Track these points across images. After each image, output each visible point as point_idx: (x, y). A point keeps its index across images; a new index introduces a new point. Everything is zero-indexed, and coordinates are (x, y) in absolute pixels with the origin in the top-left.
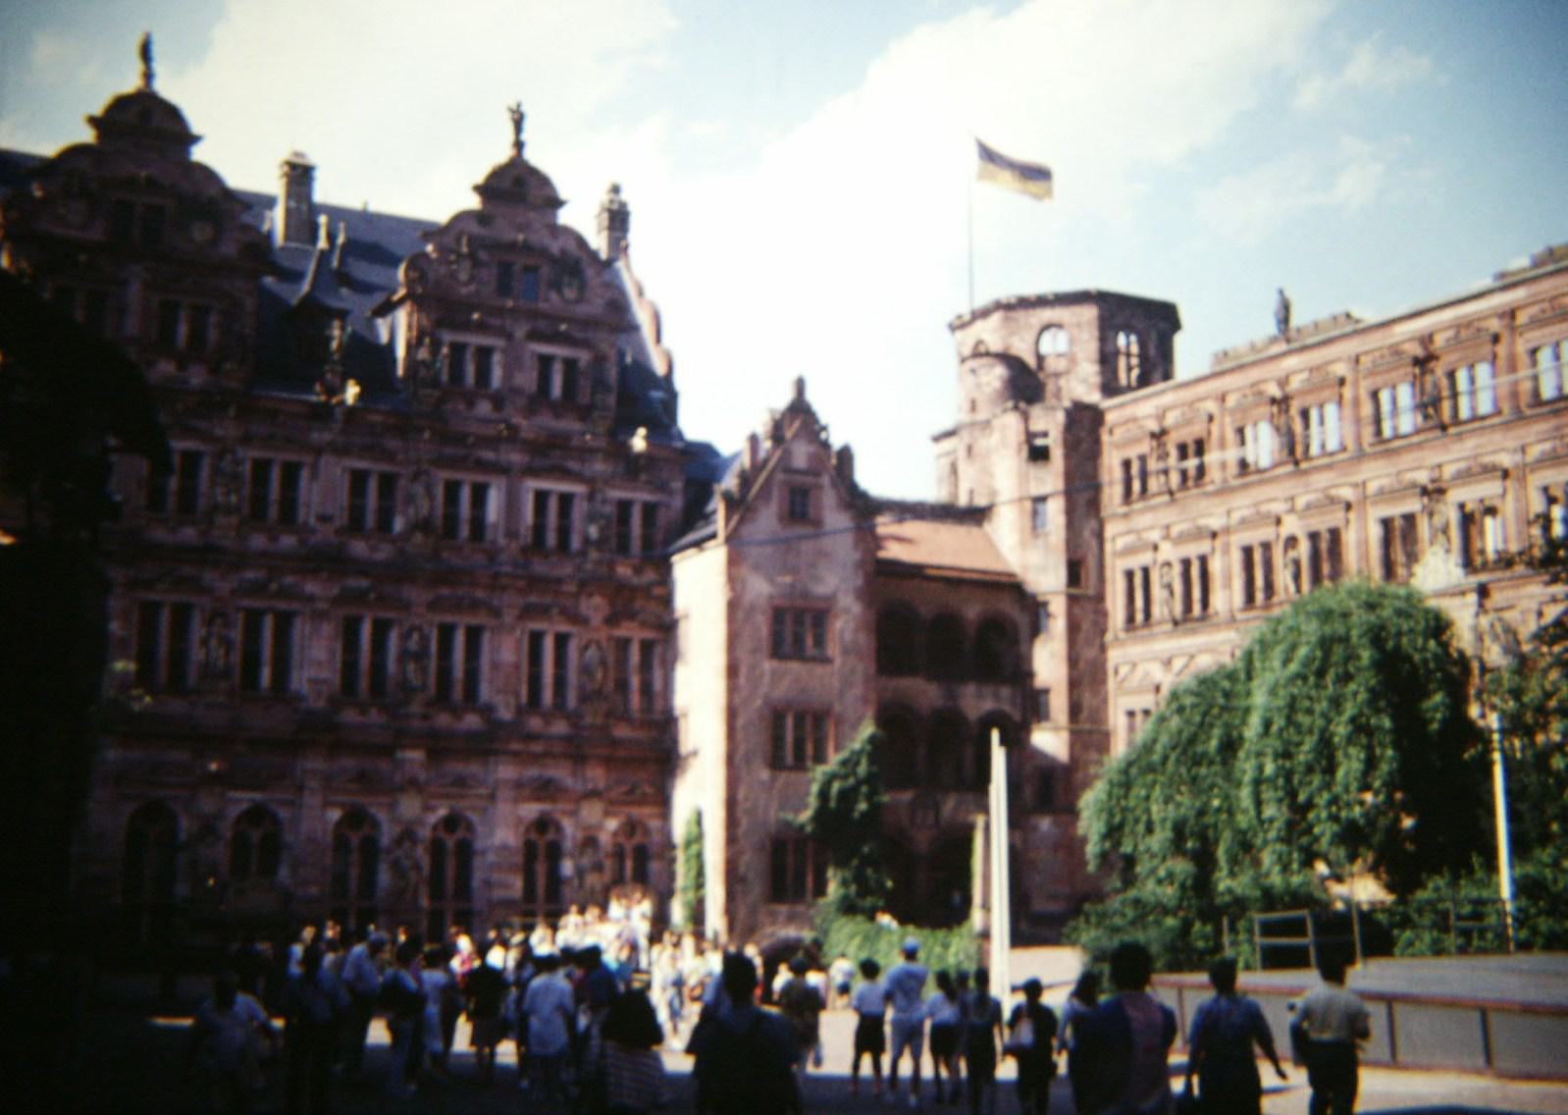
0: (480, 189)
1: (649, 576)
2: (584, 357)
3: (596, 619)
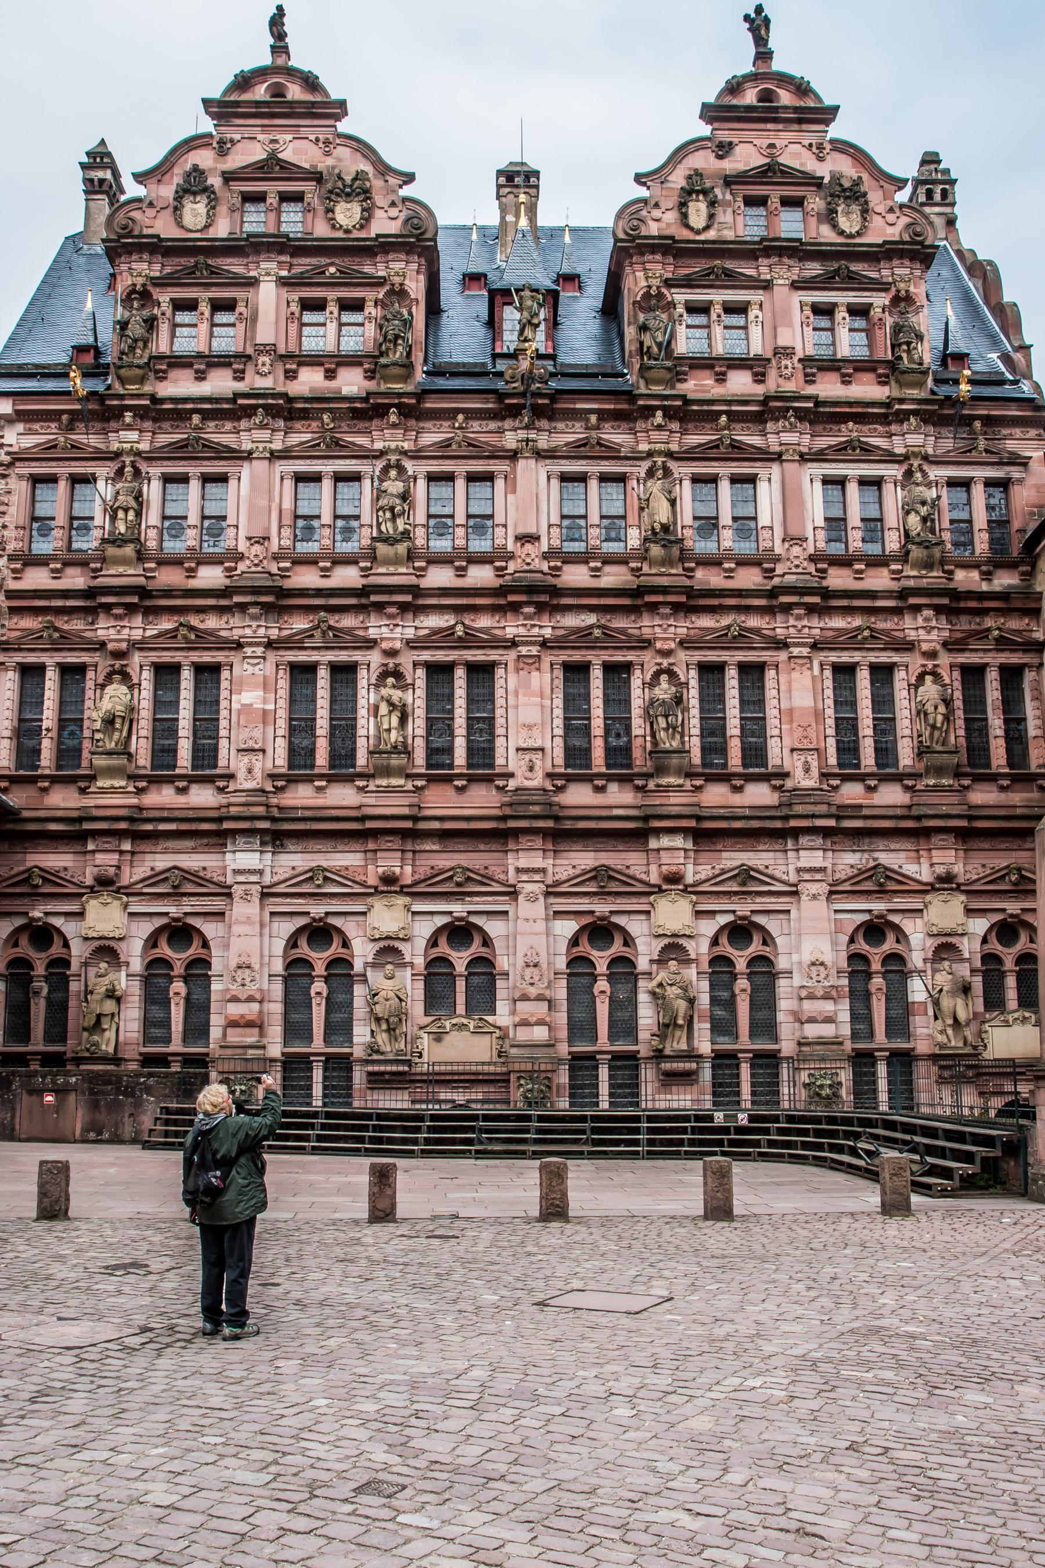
0: (711, 113)
1: (1005, 580)
2: (879, 300)
3: (930, 640)
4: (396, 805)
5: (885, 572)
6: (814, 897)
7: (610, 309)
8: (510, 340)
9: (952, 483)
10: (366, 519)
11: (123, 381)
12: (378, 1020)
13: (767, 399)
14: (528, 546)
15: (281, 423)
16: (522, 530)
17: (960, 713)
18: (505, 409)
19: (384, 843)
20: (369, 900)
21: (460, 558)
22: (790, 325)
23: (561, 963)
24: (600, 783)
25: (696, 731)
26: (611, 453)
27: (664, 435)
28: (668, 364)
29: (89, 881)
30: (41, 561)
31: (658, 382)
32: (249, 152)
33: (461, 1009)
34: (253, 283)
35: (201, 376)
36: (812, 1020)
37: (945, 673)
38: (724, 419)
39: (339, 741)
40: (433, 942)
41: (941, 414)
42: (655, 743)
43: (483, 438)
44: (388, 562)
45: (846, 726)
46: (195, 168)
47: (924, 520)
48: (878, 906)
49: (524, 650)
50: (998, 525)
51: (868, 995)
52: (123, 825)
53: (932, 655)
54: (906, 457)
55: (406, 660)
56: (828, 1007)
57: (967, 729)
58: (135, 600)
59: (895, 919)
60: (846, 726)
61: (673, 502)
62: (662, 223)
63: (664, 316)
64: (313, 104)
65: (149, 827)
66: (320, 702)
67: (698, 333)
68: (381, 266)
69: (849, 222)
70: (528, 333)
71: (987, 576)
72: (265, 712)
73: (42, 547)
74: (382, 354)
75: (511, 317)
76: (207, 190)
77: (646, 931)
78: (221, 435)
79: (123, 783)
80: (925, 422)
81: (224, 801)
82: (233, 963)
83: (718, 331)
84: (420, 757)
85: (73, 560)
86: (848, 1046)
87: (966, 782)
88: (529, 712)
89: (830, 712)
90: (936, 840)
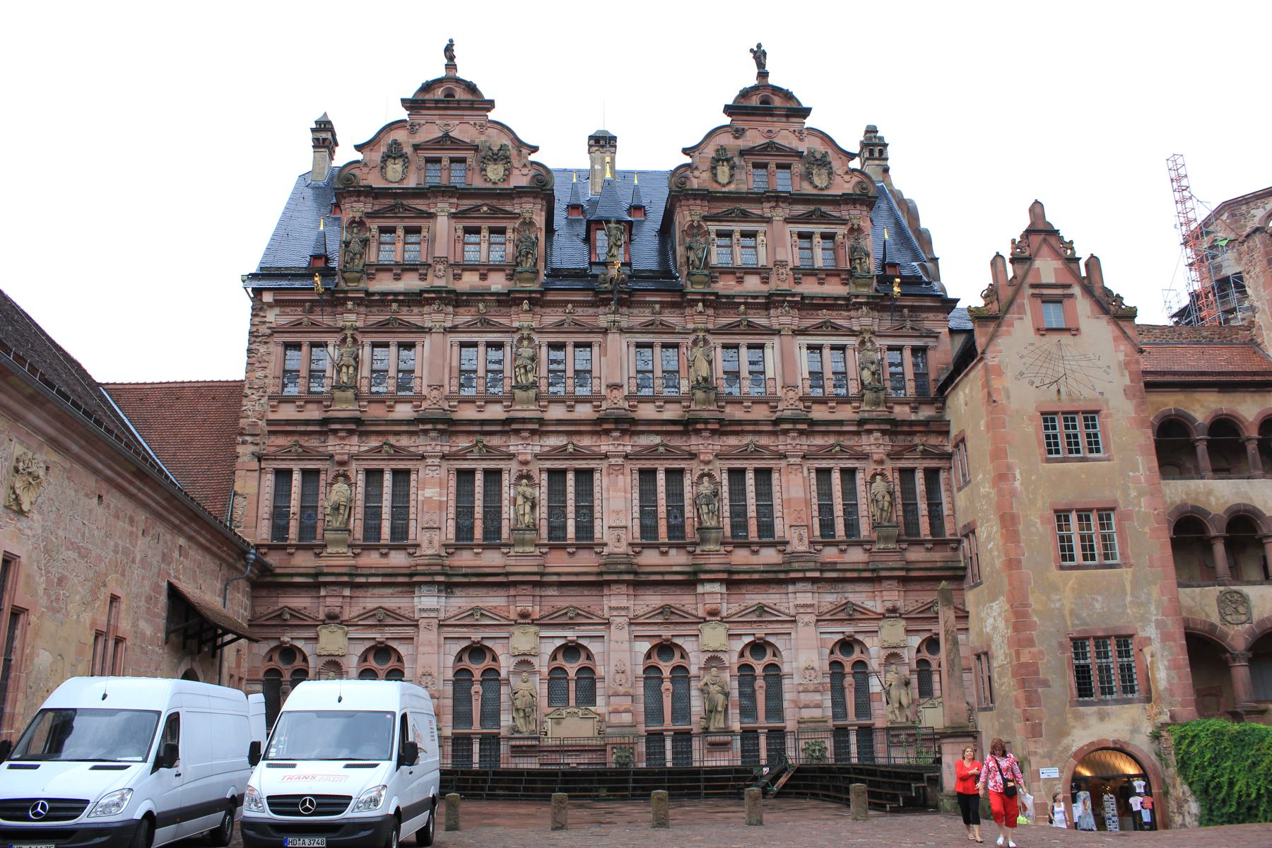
1: (926, 413)
2: (841, 231)
3: (879, 452)
4: (528, 565)
5: (848, 407)
6: (807, 624)
7: (665, 231)
8: (601, 252)
9: (890, 348)
10: (507, 373)
11: (346, 280)
12: (517, 710)
13: (769, 296)
14: (615, 392)
15: (450, 309)
16: (611, 381)
17: (899, 501)
18: (600, 300)
19: (521, 590)
20: (511, 629)
21: (570, 400)
22: (784, 246)
23: (640, 670)
24: (664, 549)
25: (727, 514)
26: (670, 330)
27: (703, 318)
28: (706, 272)
29: (322, 617)
30: (290, 400)
31: (699, 283)
32: (430, 132)
33: (572, 702)
34: (432, 216)
35: (397, 278)
36: (806, 706)
37: (889, 474)
38: (742, 307)
39: (489, 522)
40: (554, 657)
41: (880, 304)
42: (700, 522)
43: (584, 319)
44: (522, 402)
45: (826, 510)
46: (395, 142)
47: (873, 374)
48: (849, 629)
49: (613, 461)
50: (920, 377)
51: (843, 689)
52: (346, 579)
53: (881, 462)
54: (861, 333)
55: (534, 468)
56: (817, 697)
57: (904, 511)
58: (353, 427)
59: (860, 637)
60: (826, 510)
61: (710, 363)
62: (700, 180)
63: (702, 240)
64: (473, 102)
65: (363, 580)
66: (477, 496)
67: (724, 250)
68: (517, 206)
69: (820, 180)
70: (614, 251)
71: (915, 410)
72: (441, 502)
73: (292, 390)
74: (517, 265)
75: (600, 237)
76: (403, 156)
77: (695, 648)
78: (413, 316)
79: (345, 550)
80: (872, 309)
81: (413, 563)
82: (420, 672)
83: (737, 250)
84: (544, 532)
85: (312, 398)
86: (831, 723)
87: (904, 546)
88: (616, 502)
89: (815, 501)
90: (886, 584)
